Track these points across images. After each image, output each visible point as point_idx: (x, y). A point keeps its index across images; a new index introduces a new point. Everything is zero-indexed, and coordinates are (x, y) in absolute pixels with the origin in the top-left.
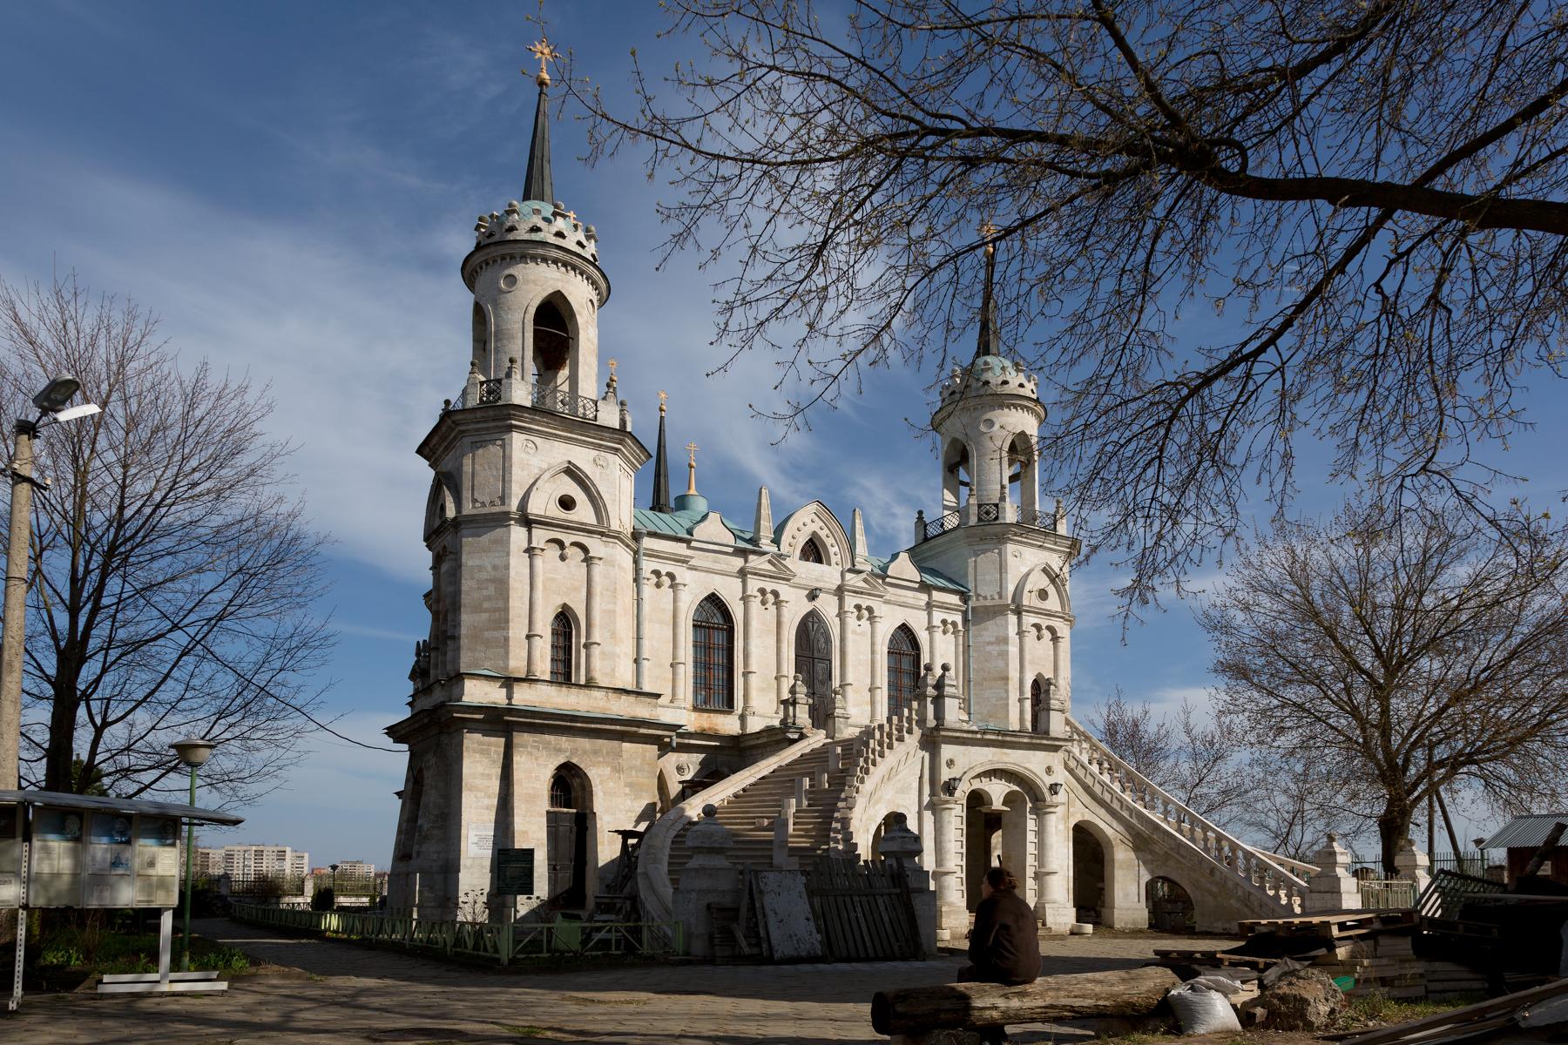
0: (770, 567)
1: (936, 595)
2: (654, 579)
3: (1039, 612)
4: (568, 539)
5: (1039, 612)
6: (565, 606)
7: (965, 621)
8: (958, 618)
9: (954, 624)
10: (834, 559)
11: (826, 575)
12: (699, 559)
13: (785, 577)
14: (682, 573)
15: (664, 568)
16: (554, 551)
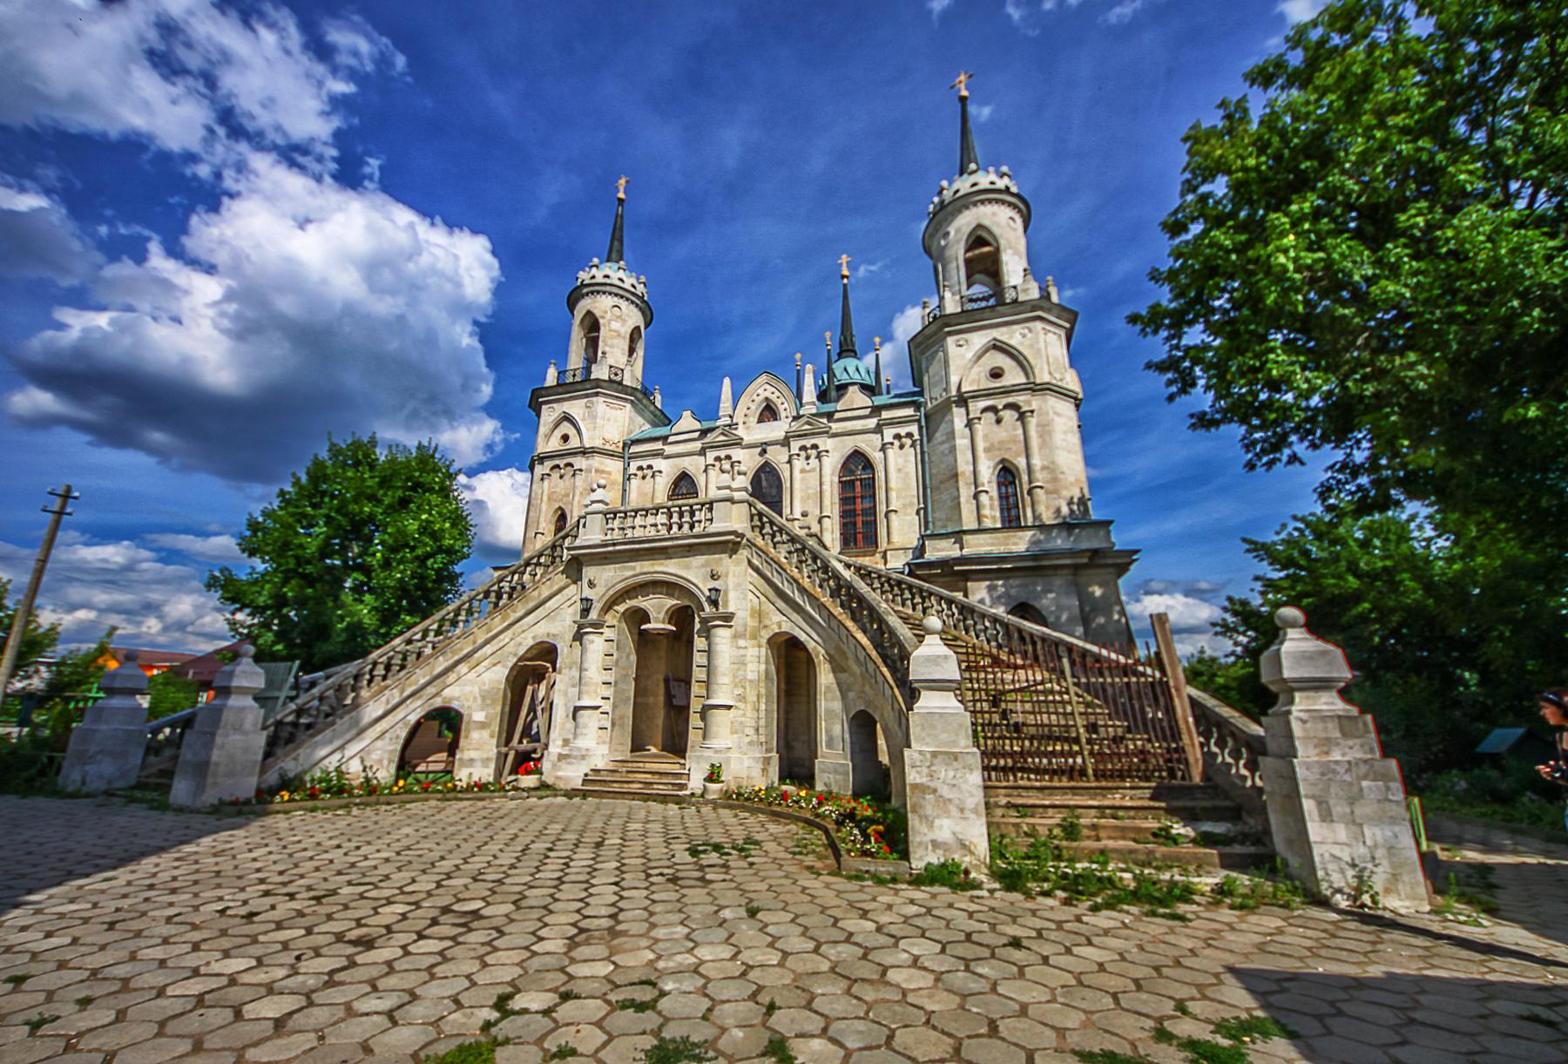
0: (722, 438)
1: (885, 414)
2: (640, 473)
3: (988, 393)
4: (562, 463)
5: (988, 393)
6: (560, 508)
7: (920, 428)
8: (914, 429)
9: (909, 435)
10: (783, 414)
11: (776, 430)
12: (669, 450)
13: (738, 443)
14: (658, 463)
15: (644, 464)
16: (556, 475)
